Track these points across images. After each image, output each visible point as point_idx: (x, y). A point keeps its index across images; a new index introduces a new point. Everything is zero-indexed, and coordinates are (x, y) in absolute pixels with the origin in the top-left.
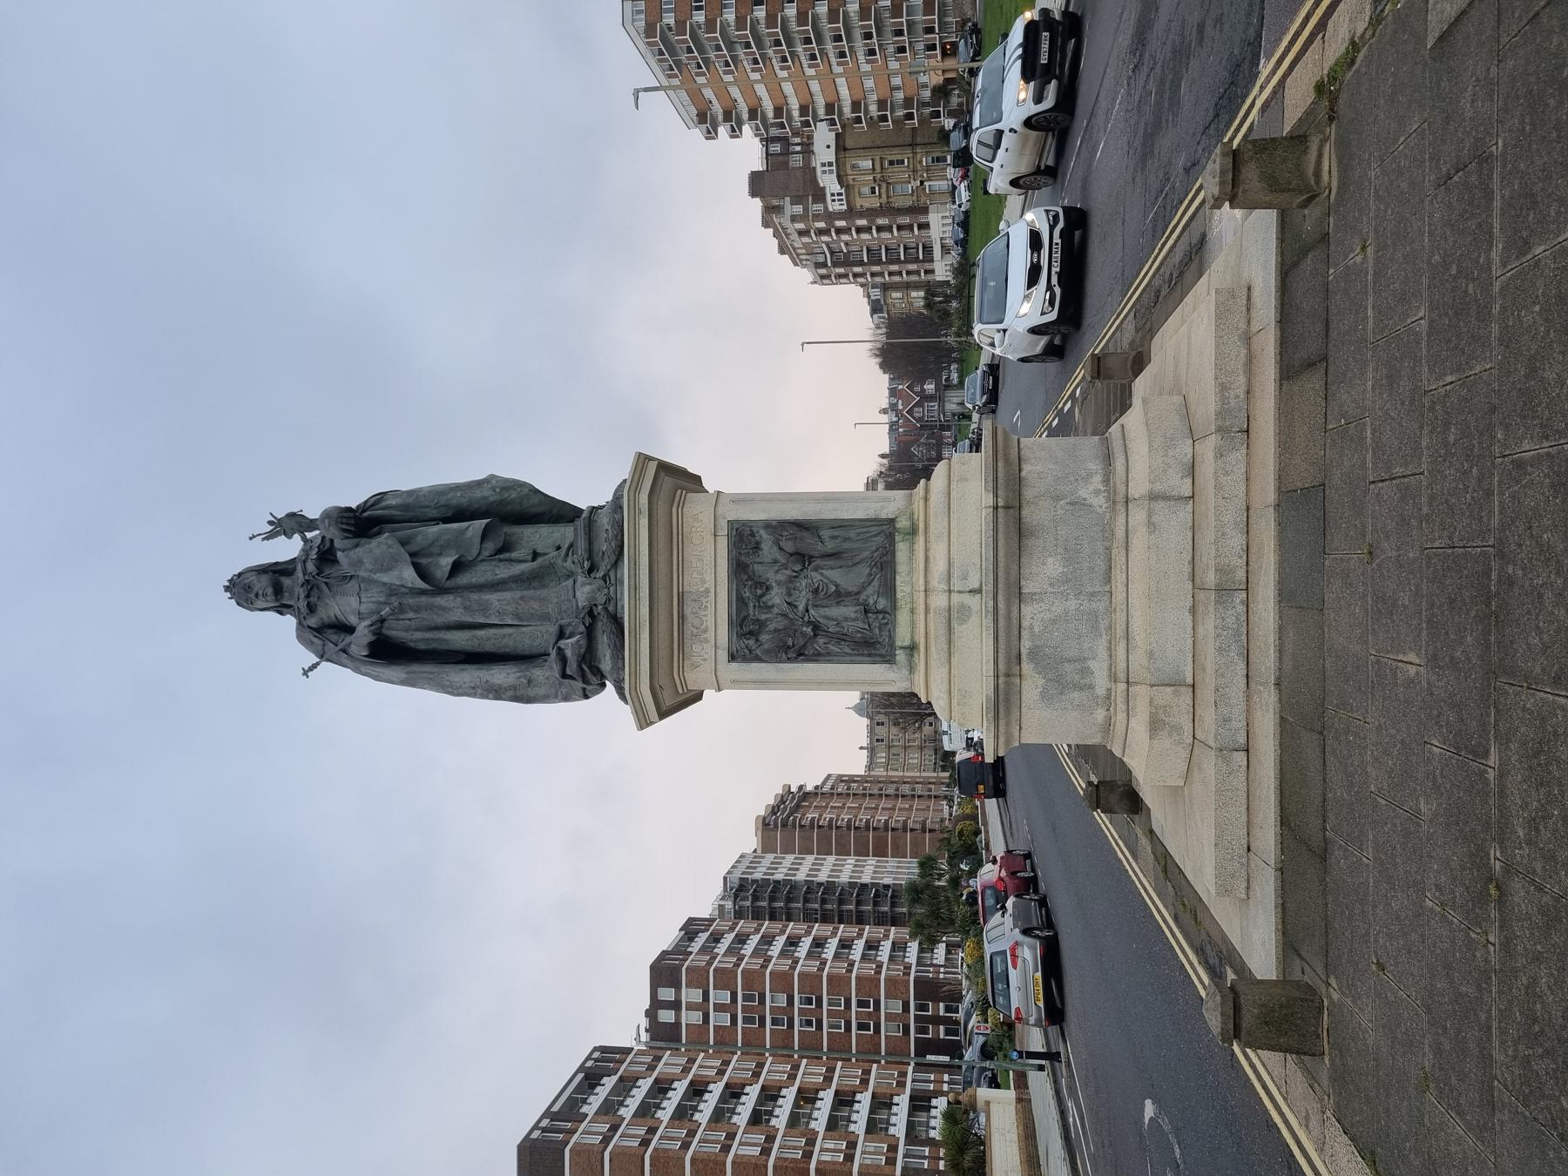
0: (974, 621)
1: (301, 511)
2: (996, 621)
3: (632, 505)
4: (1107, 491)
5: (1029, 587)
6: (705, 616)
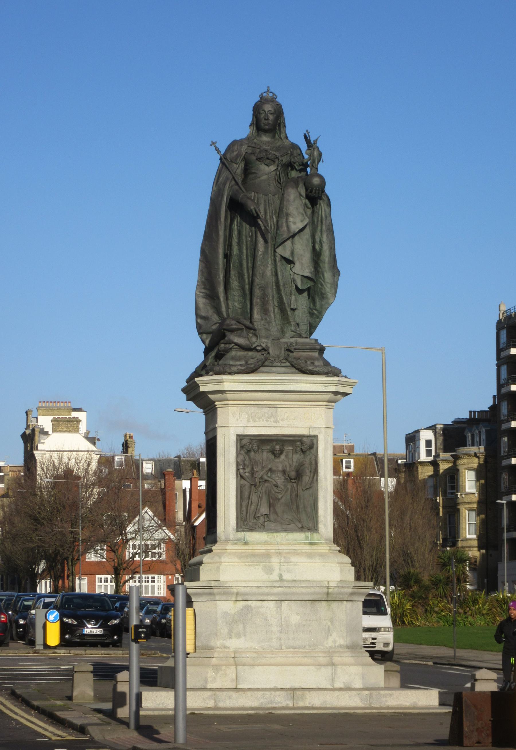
0: (265, 577)
1: (323, 162)
2: (267, 587)
3: (329, 382)
4: (335, 647)
5: (284, 604)
6: (263, 421)
